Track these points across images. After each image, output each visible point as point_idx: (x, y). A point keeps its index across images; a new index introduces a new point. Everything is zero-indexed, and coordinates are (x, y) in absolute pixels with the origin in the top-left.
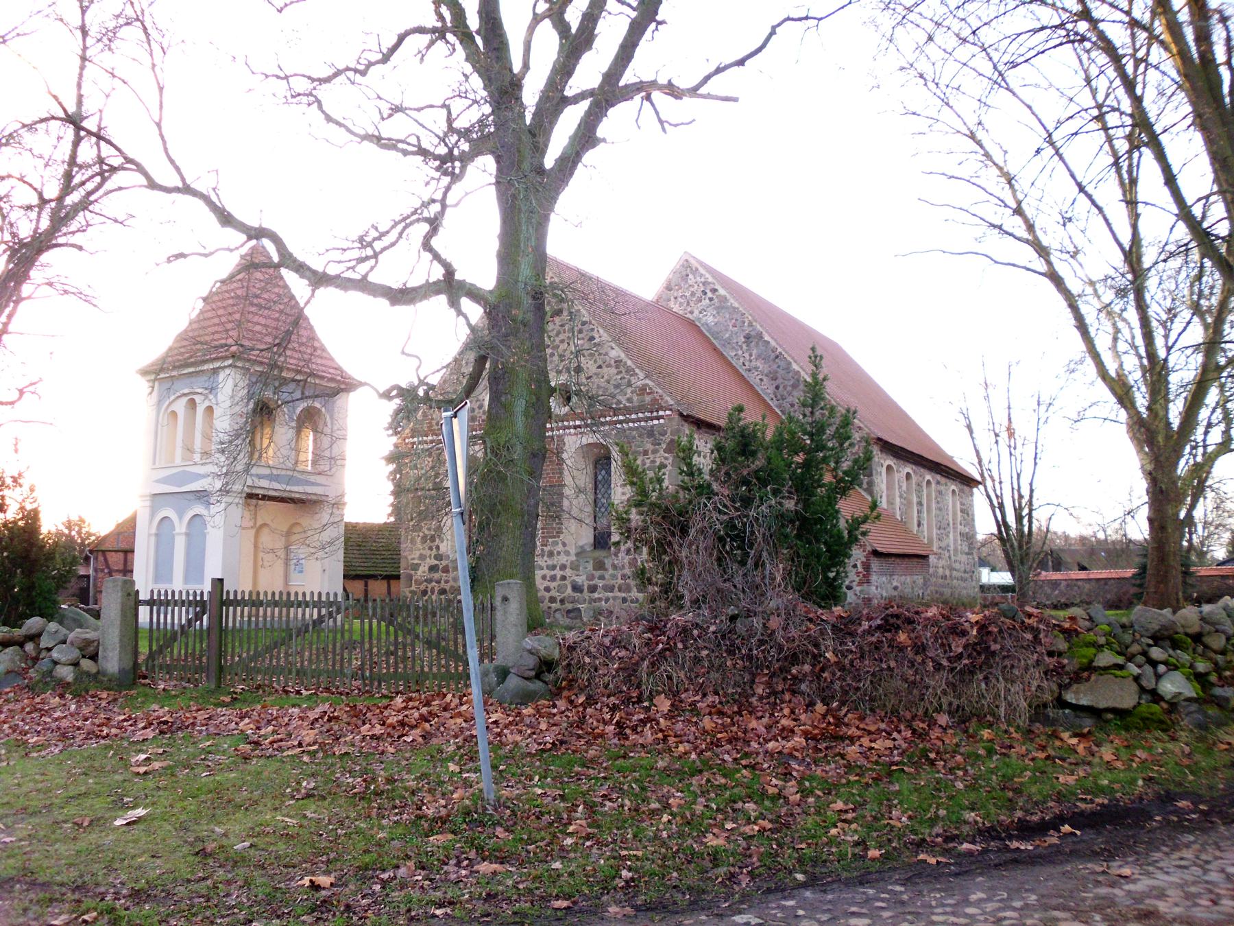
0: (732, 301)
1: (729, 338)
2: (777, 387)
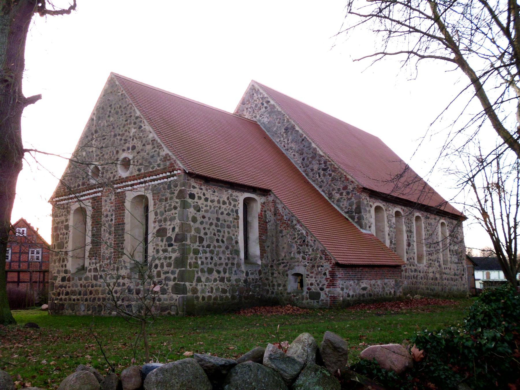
0: (278, 107)
1: (276, 131)
2: (303, 159)
